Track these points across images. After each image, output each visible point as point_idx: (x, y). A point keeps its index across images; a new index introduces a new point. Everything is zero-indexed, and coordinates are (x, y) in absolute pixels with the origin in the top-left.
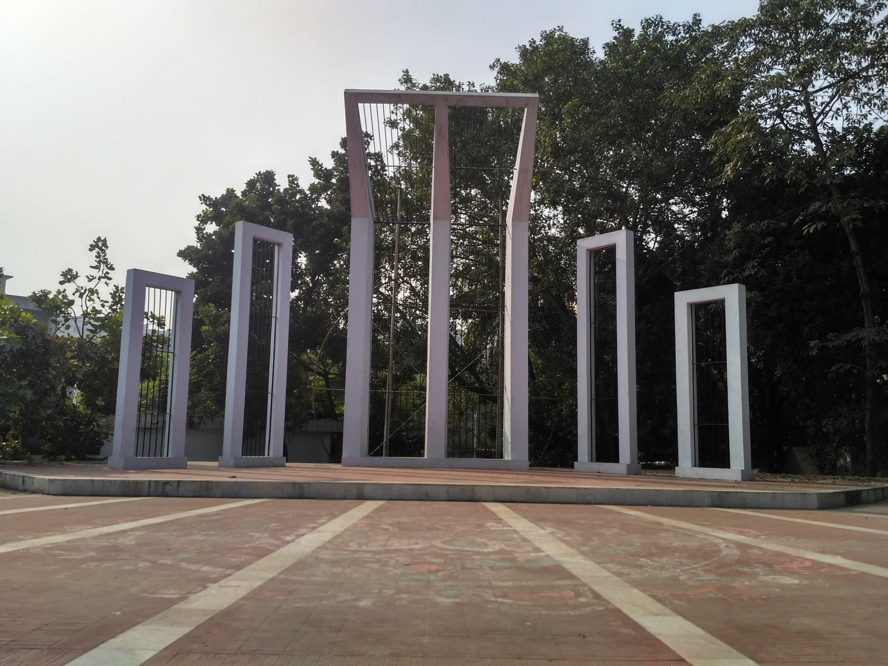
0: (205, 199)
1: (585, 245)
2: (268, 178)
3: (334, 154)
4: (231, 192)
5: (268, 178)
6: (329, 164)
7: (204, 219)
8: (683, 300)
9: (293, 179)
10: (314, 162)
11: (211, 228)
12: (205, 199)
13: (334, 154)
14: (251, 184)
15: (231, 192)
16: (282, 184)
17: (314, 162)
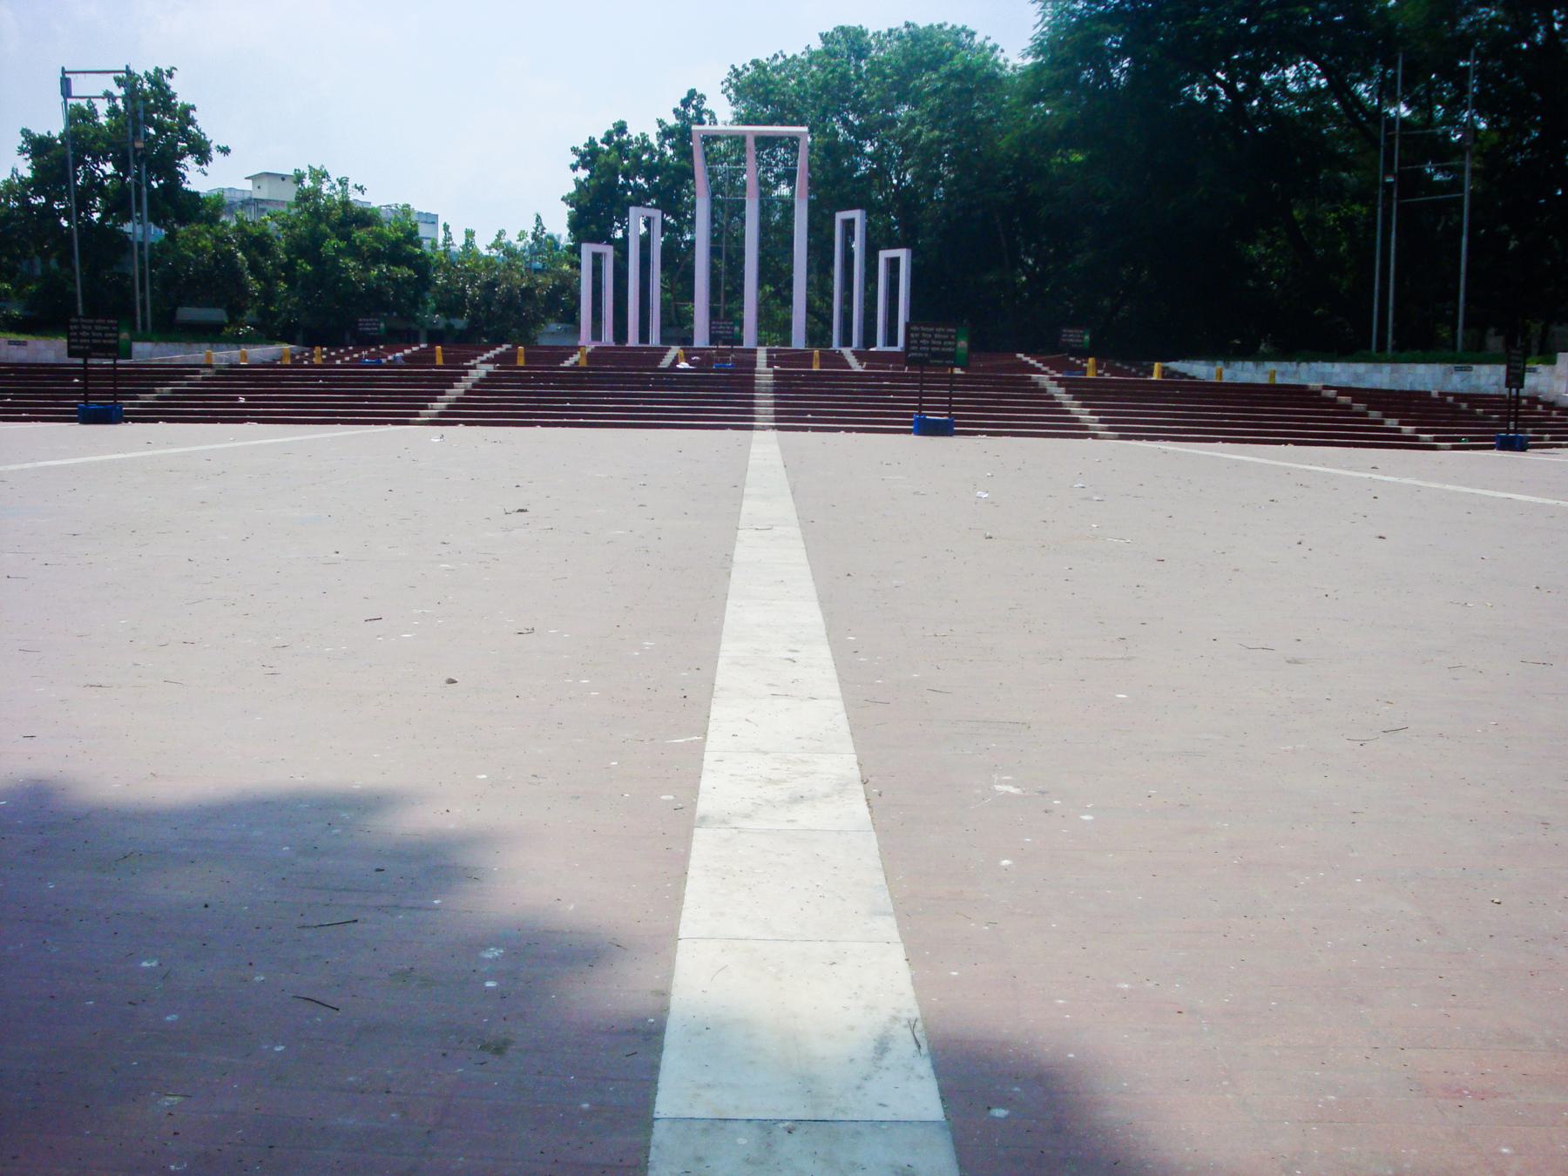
0: (575, 150)
1: (840, 216)
2: (621, 128)
3: (675, 111)
4: (592, 141)
5: (621, 128)
6: (672, 121)
7: (574, 168)
8: (884, 255)
9: (645, 137)
10: (661, 123)
11: (583, 174)
12: (575, 150)
13: (675, 111)
14: (609, 136)
15: (592, 141)
16: (634, 132)
17: (661, 123)
